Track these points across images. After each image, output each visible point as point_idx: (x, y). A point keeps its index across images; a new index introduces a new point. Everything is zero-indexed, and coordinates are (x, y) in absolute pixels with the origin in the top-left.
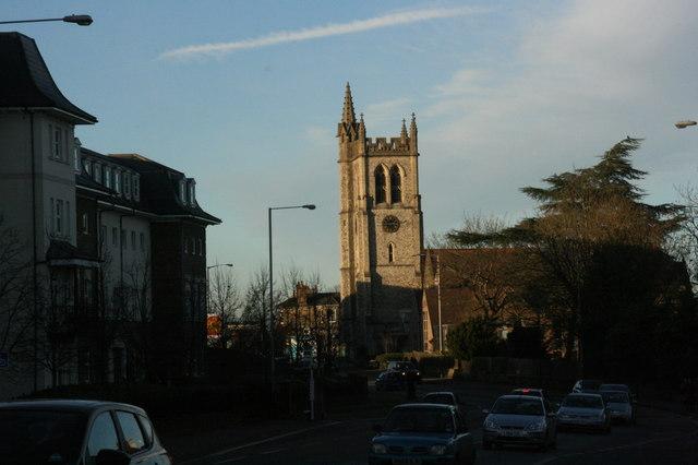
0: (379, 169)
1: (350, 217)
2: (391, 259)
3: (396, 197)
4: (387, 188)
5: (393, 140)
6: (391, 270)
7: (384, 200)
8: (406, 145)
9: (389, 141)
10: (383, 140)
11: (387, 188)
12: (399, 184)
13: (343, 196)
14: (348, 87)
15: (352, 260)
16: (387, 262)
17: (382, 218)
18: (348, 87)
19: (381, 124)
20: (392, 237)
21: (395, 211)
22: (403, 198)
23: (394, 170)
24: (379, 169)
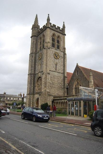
0: (54, 35)
2: (56, 70)
3: (58, 47)
4: (56, 44)
6: (56, 74)
8: (62, 31)
10: (54, 26)
11: (56, 44)
12: (59, 43)
14: (37, 15)
15: (35, 71)
16: (55, 70)
17: (54, 52)
18: (37, 15)
19: (57, 22)
20: (57, 61)
21: (58, 51)
22: (60, 48)
23: (59, 37)
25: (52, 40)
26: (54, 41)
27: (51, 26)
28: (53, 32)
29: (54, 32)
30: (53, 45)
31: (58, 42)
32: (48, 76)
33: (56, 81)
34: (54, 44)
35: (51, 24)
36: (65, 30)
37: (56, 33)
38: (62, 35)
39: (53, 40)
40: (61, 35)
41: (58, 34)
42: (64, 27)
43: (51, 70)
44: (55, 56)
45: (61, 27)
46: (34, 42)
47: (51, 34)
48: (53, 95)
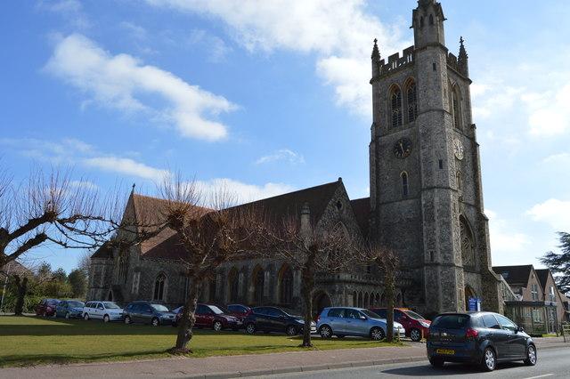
0: (395, 89)
3: (413, 115)
5: (406, 52)
9: (401, 55)
10: (394, 58)
24: (395, 89)
27: (384, 66)
28: (389, 80)
30: (396, 122)
31: (412, 97)
34: (400, 114)
39: (395, 103)
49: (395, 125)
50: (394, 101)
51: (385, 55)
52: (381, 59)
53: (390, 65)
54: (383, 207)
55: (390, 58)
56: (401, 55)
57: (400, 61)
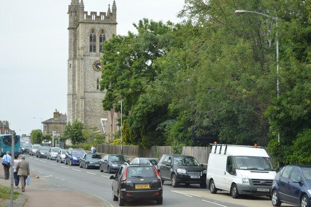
0: (93, 30)
1: (73, 62)
5: (101, 13)
7: (95, 50)
9: (98, 14)
10: (95, 13)
13: (70, 50)
17: (93, 62)
23: (103, 31)
24: (93, 30)
25: (91, 40)
26: (95, 40)
28: (90, 26)
29: (93, 25)
32: (80, 102)
33: (98, 106)
34: (95, 47)
35: (86, 13)
36: (116, 15)
37: (98, 28)
38: (110, 26)
39: (92, 39)
40: (106, 26)
41: (101, 26)
42: (115, 9)
43: (89, 91)
44: (95, 68)
45: (111, 11)
46: (70, 39)
47: (88, 31)
48: (93, 127)
49: (91, 50)
50: (91, 37)
51: (88, 9)
52: (85, 10)
53: (90, 17)
54: (87, 94)
55: (92, 13)
56: (98, 14)
57: (97, 17)
